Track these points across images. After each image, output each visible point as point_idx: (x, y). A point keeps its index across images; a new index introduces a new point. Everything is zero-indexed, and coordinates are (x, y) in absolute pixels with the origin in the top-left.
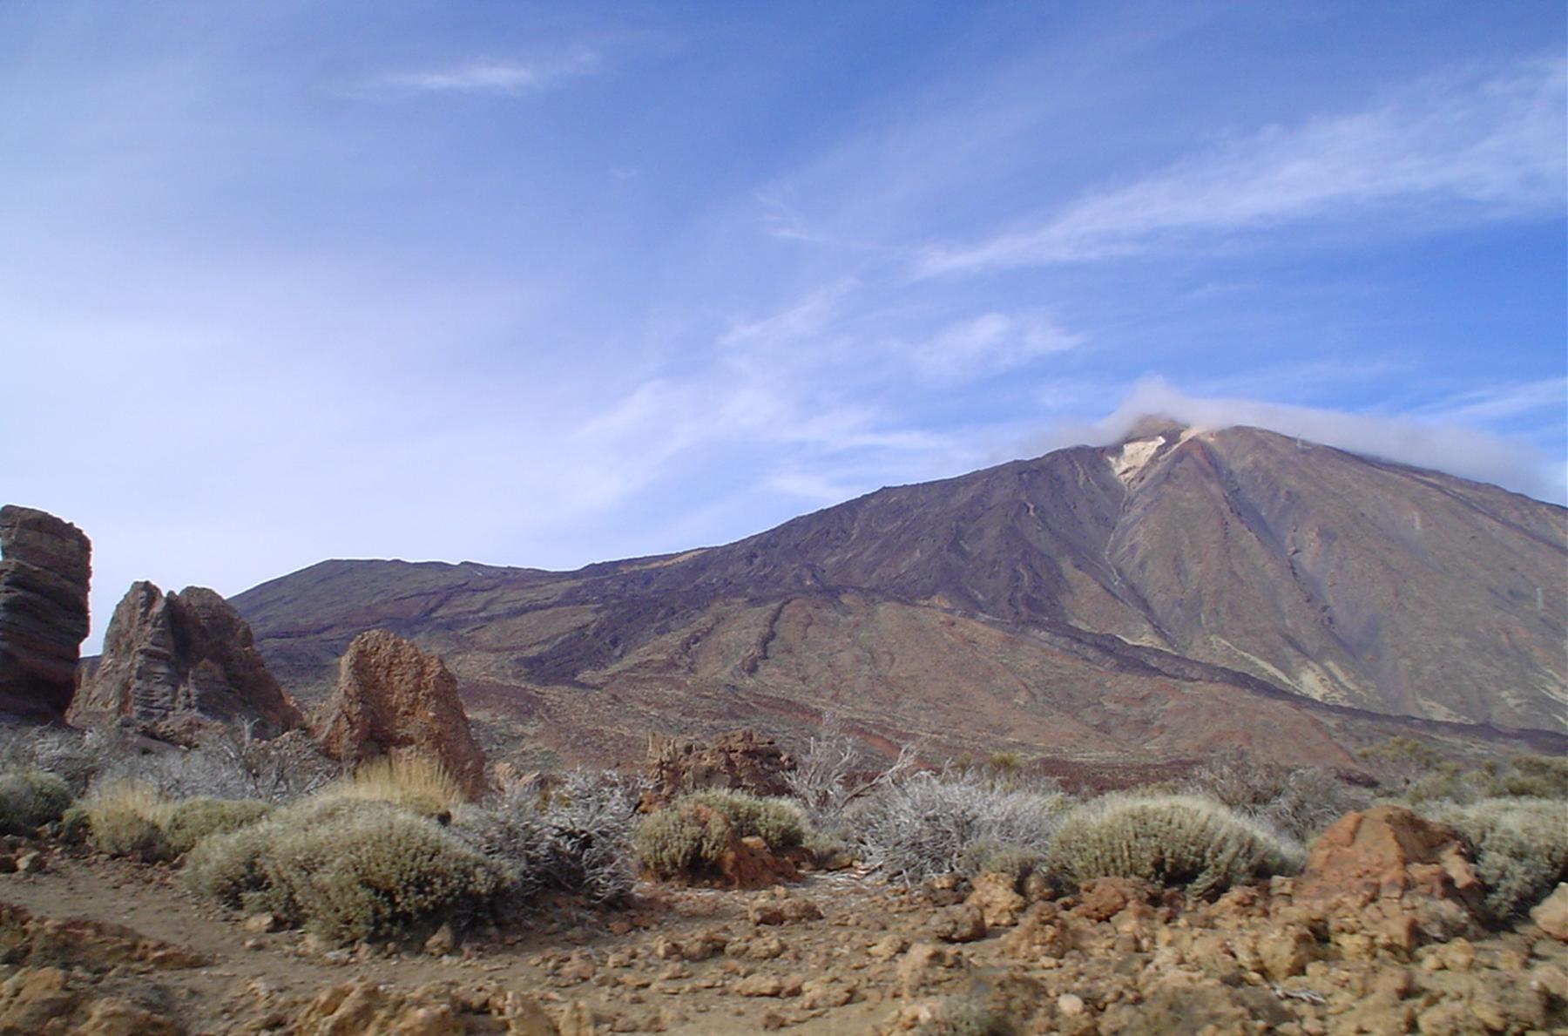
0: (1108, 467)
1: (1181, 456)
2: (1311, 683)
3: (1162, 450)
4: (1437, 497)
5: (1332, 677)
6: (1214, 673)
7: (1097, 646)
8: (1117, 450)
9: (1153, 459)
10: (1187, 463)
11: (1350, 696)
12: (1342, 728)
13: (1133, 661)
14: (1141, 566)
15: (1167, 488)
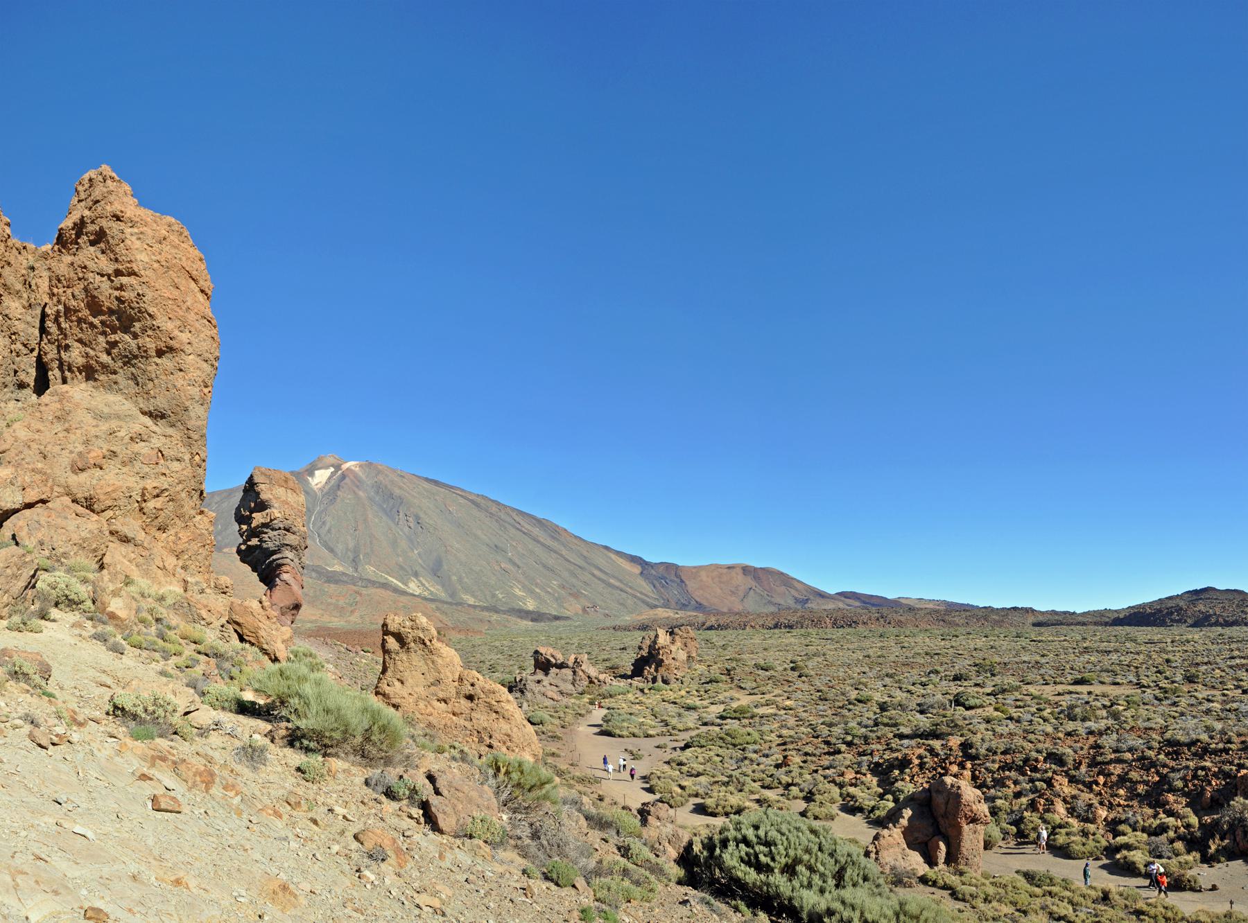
0: (307, 481)
1: (343, 477)
2: (413, 587)
3: (333, 474)
4: (462, 501)
5: (423, 585)
6: (373, 583)
7: (317, 572)
8: (311, 473)
9: (330, 478)
10: (347, 480)
11: (432, 593)
12: (438, 609)
13: (332, 578)
14: (329, 531)
15: (339, 493)
